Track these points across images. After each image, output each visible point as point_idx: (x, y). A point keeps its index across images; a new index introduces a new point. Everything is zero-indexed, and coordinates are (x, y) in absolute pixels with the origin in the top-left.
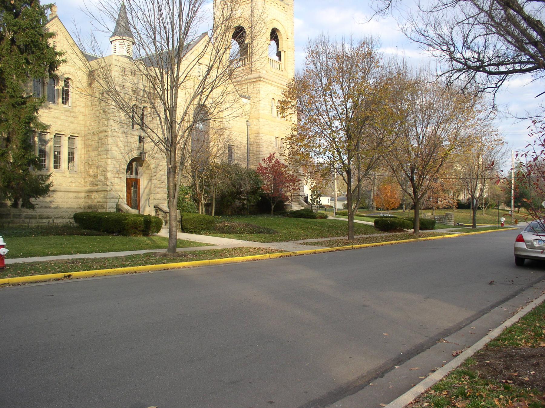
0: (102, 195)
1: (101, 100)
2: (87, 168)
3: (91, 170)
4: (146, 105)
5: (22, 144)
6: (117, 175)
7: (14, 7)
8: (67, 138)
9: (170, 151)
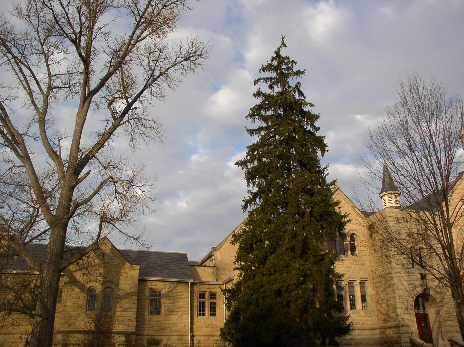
0: (395, 331)
1: (382, 248)
2: (379, 307)
4: (421, 245)
5: (325, 293)
6: (406, 312)
7: (310, 189)
8: (358, 283)
9: (456, 286)
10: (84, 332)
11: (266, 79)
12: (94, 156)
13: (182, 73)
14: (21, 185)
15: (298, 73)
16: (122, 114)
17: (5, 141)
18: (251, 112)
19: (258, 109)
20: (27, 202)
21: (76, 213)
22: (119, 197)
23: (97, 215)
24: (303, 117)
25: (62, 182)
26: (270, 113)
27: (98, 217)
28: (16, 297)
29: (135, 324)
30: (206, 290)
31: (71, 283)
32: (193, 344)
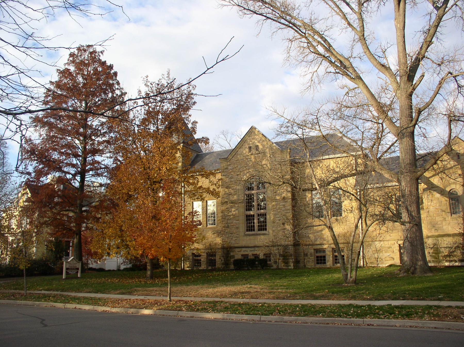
10: (454, 235)
12: (424, 57)
14: (360, 105)
17: (335, 70)
20: (371, 119)
21: (419, 120)
23: (443, 116)
25: (398, 92)
27: (445, 117)
28: (385, 207)
31: (429, 189)
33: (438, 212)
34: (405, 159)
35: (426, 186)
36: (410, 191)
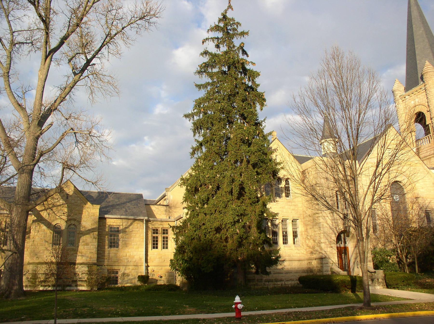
3: (310, 243)
11: (213, 39)
12: (56, 109)
13: (137, 32)
15: (243, 34)
16: (82, 69)
18: (199, 69)
19: (205, 66)
21: (41, 159)
22: (80, 145)
24: (245, 74)
26: (215, 70)
29: (96, 256)
30: (159, 226)
32: (148, 273)
33: (42, 242)
34: (20, 192)
35: (36, 218)
36: (19, 222)
